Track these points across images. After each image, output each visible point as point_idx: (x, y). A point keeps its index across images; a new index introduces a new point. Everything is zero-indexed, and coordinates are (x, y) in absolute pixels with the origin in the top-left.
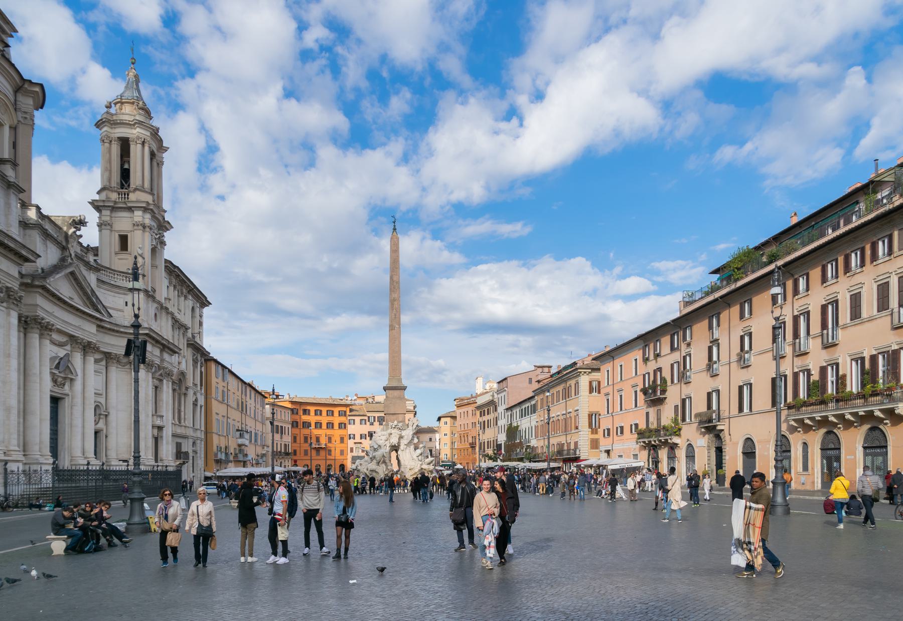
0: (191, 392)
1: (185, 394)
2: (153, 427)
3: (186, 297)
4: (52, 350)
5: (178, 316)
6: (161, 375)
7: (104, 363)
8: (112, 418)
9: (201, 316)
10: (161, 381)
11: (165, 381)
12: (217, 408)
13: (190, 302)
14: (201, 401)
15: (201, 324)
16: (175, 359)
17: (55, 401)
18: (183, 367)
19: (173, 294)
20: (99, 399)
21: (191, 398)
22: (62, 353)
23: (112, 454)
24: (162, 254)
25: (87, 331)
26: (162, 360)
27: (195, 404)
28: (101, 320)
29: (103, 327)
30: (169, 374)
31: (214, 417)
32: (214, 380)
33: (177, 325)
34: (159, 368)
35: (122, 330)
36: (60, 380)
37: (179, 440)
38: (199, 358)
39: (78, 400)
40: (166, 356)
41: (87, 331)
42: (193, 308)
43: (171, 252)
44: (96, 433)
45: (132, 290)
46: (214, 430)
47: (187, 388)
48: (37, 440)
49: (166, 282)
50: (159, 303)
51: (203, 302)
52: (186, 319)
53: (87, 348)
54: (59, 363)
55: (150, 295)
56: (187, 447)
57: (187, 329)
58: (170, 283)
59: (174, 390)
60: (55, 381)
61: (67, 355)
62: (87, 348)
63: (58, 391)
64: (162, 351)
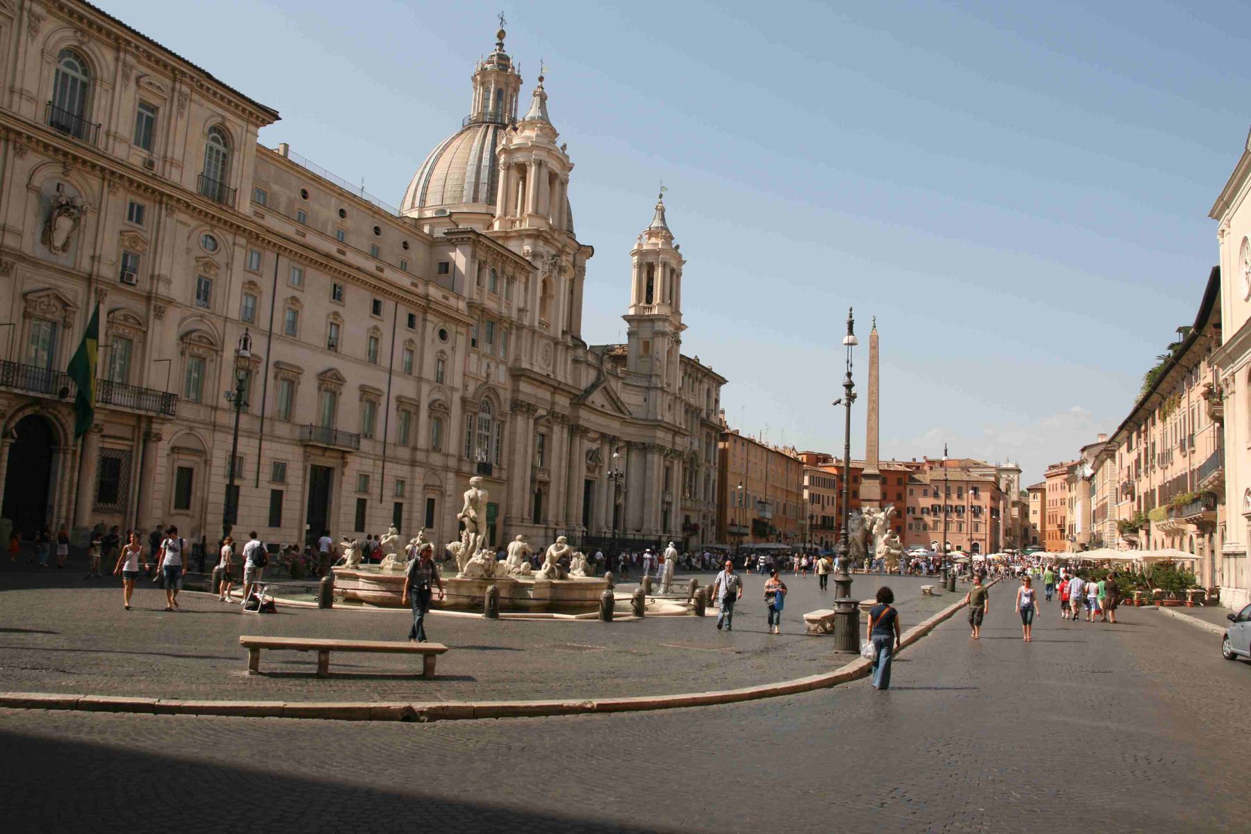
2: (663, 502)
4: (587, 445)
5: (692, 401)
9: (718, 395)
10: (672, 463)
14: (714, 475)
16: (687, 440)
17: (588, 483)
22: (595, 446)
23: (630, 526)
24: (677, 350)
26: (674, 443)
30: (680, 454)
33: (691, 411)
34: (673, 451)
38: (713, 434)
40: (678, 439)
41: (614, 428)
42: (709, 391)
45: (648, 388)
46: (729, 502)
49: (680, 374)
50: (674, 394)
51: (721, 381)
52: (699, 401)
53: (612, 440)
58: (685, 373)
59: (685, 469)
60: (588, 469)
63: (591, 476)
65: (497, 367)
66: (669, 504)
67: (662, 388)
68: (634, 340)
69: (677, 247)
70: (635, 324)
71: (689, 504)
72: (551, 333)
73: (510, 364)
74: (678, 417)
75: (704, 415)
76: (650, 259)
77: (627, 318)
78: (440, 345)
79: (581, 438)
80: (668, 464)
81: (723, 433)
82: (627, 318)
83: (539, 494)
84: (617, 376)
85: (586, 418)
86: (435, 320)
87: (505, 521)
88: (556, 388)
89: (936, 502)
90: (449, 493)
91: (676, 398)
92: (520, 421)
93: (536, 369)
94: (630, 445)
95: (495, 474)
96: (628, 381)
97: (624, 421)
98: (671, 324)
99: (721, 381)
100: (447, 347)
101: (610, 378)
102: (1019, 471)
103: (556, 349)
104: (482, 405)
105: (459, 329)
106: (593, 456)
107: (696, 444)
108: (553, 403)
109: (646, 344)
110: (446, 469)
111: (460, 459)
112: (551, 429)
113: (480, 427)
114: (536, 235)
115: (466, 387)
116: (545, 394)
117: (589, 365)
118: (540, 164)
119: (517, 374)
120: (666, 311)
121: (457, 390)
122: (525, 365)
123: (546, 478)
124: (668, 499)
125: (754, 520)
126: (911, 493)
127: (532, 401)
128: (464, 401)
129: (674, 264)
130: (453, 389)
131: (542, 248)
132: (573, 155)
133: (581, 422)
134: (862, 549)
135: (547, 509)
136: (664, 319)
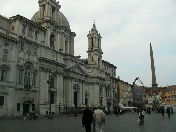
1: (110, 89)
2: (100, 97)
3: (109, 68)
4: (74, 83)
5: (107, 72)
6: (102, 86)
7: (88, 84)
8: (90, 96)
11: (103, 87)
12: (121, 92)
13: (111, 69)
14: (116, 90)
15: (115, 73)
18: (109, 83)
21: (112, 90)
22: (76, 83)
25: (83, 78)
27: (114, 91)
28: (86, 75)
30: (104, 85)
31: (121, 94)
32: (120, 85)
33: (107, 74)
35: (91, 77)
37: (108, 100)
39: (81, 92)
40: (103, 81)
41: (83, 78)
42: (112, 70)
43: (103, 59)
45: (93, 68)
47: (111, 88)
48: (70, 101)
49: (103, 65)
51: (115, 68)
52: (110, 72)
53: (83, 81)
54: (76, 85)
57: (110, 74)
59: (106, 89)
60: (75, 89)
62: (83, 81)
63: (76, 91)
65: (33, 57)
66: (102, 98)
67: (96, 68)
68: (89, 57)
69: (100, 34)
71: (108, 98)
72: (55, 49)
73: (39, 56)
74: (103, 76)
75: (111, 75)
76: (92, 36)
77: (87, 52)
78: (5, 48)
79: (71, 81)
80: (100, 87)
81: (118, 80)
82: (87, 52)
83: (52, 95)
84: (83, 65)
85: (71, 75)
86: (2, 40)
87: (38, 103)
88: (57, 64)
89: (172, 95)
90: (10, 94)
91: (102, 71)
92: (42, 73)
93: (48, 58)
94: (89, 82)
95: (33, 89)
96: (86, 66)
97: (86, 77)
98: (98, 52)
99: (115, 68)
100: (8, 48)
101: (80, 65)
103: (57, 54)
104: (25, 68)
105: (14, 43)
108: (57, 69)
109: (93, 58)
110: (9, 87)
111: (16, 84)
112: (56, 77)
113: (25, 74)
114: (47, 21)
115: (19, 62)
116: (54, 67)
117: (72, 61)
118: (48, 4)
119: (42, 60)
120: (97, 49)
121: (13, 62)
122: (43, 56)
123: (54, 90)
124: (101, 96)
125: (128, 101)
126: (166, 93)
127: (48, 68)
128: (18, 66)
129: (98, 38)
130: (11, 61)
131: (49, 25)
132: (60, 3)
133: (71, 76)
134: (154, 106)
135: (56, 100)
136: (96, 51)
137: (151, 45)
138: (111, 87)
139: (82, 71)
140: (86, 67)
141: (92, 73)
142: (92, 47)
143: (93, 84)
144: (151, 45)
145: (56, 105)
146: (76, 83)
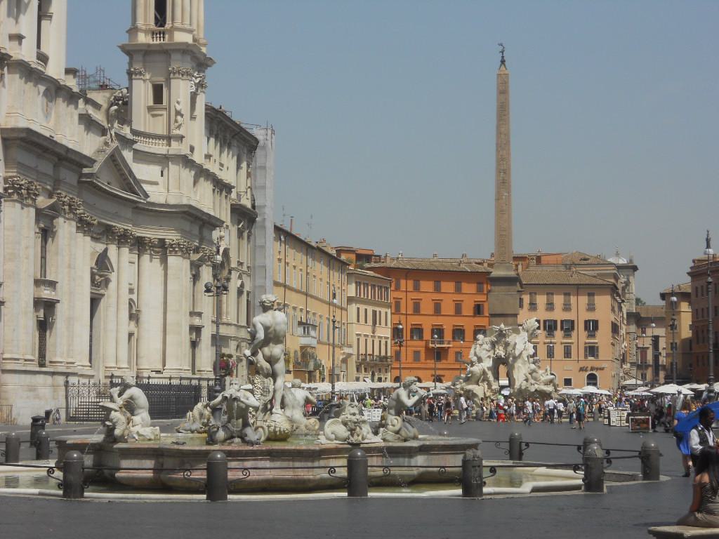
0: (234, 275)
17: (95, 302)
19: (212, 147)
20: (131, 296)
22: (100, 247)
29: (137, 208)
33: (222, 187)
36: (97, 277)
39: (113, 300)
44: (131, 335)
52: (228, 176)
55: (187, 162)
56: (230, 349)
61: (106, 250)
62: (122, 239)
64: (201, 228)
70: (138, 57)
74: (204, 199)
75: (234, 195)
102: (635, 268)
106: (102, 262)
107: (226, 239)
124: (197, 321)
137: (503, 62)
138: (234, 265)
139: (126, 179)
140: (142, 157)
141: (156, 183)
142: (156, 24)
143: (163, 249)
144: (503, 62)
145: (53, 374)
146: (100, 247)
